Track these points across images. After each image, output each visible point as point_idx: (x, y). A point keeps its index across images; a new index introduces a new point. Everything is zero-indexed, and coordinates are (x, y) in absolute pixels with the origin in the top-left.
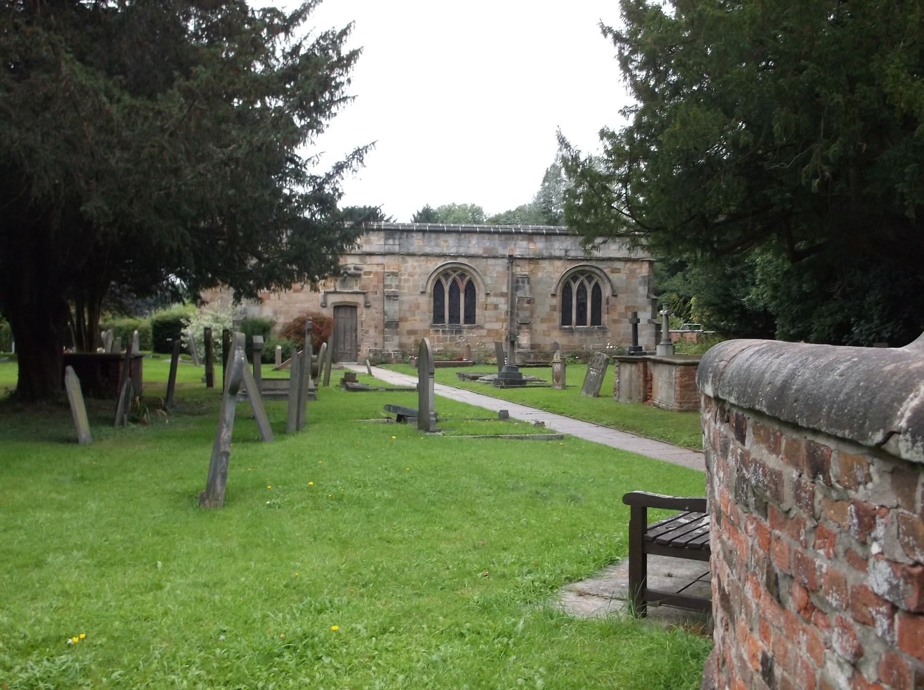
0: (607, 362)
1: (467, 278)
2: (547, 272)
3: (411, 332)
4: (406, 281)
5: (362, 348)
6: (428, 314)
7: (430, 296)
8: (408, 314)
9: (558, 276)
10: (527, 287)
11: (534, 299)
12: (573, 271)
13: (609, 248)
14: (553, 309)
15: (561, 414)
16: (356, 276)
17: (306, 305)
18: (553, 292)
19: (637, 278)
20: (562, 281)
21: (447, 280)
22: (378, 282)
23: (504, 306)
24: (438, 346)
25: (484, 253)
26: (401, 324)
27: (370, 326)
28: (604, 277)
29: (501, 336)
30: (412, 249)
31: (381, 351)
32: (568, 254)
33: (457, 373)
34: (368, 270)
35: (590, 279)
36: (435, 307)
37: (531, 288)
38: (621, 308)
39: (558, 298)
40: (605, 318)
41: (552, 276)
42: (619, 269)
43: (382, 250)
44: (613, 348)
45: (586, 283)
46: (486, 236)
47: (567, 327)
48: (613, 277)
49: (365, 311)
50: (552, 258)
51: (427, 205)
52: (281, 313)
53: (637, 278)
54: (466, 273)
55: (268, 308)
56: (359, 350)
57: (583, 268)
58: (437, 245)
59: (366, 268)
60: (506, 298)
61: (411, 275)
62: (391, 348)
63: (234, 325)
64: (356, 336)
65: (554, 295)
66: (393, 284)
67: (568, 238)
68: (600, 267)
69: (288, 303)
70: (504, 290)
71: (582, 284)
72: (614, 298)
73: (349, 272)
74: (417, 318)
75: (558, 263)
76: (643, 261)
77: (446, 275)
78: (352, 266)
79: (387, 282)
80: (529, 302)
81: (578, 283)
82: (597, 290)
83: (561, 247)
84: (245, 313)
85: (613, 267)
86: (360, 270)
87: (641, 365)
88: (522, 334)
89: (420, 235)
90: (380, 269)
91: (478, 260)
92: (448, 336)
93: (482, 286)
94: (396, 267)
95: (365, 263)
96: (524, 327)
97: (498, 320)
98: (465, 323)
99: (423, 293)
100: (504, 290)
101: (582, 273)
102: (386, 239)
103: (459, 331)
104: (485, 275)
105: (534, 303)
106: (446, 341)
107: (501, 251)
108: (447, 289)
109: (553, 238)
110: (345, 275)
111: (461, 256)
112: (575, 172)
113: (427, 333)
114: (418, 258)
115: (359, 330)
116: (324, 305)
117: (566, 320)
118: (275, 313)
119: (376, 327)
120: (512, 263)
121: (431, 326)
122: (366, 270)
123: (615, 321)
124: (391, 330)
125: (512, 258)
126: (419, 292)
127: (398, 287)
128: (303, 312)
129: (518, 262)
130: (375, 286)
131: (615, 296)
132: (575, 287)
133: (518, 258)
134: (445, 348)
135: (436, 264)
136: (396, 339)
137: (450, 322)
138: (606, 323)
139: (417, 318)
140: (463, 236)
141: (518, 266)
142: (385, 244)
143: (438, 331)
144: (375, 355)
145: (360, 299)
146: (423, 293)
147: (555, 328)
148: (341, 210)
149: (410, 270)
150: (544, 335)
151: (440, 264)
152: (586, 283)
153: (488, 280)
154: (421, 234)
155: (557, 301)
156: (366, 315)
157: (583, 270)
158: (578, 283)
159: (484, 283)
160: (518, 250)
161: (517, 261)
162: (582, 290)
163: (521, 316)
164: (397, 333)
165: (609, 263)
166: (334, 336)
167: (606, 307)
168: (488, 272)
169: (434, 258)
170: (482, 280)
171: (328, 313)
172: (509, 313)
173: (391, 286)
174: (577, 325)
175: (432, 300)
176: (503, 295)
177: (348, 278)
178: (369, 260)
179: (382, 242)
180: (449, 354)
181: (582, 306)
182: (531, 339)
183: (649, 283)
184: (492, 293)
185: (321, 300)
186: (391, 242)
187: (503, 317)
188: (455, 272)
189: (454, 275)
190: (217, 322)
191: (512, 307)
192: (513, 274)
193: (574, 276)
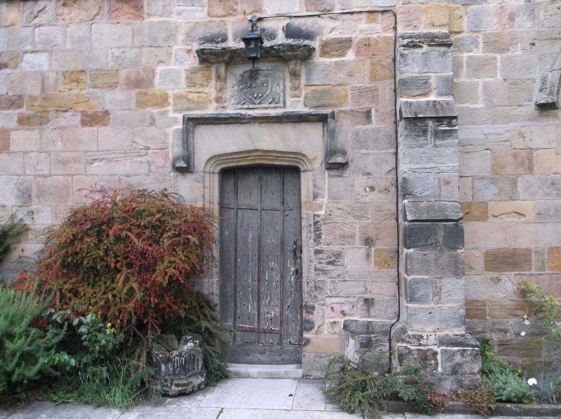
5: (316, 317)
22: (374, 78)
34: (335, 35)
52: (41, 194)
56: (307, 325)
64: (298, 273)
69: (65, 163)
86: (309, 36)
115: (307, 253)
119: (368, 241)
122: (327, 36)
124: (431, 254)
126: (531, 108)
130: (361, 92)
144: (367, 345)
156: (334, 198)
166: (222, 272)
177: (263, 66)
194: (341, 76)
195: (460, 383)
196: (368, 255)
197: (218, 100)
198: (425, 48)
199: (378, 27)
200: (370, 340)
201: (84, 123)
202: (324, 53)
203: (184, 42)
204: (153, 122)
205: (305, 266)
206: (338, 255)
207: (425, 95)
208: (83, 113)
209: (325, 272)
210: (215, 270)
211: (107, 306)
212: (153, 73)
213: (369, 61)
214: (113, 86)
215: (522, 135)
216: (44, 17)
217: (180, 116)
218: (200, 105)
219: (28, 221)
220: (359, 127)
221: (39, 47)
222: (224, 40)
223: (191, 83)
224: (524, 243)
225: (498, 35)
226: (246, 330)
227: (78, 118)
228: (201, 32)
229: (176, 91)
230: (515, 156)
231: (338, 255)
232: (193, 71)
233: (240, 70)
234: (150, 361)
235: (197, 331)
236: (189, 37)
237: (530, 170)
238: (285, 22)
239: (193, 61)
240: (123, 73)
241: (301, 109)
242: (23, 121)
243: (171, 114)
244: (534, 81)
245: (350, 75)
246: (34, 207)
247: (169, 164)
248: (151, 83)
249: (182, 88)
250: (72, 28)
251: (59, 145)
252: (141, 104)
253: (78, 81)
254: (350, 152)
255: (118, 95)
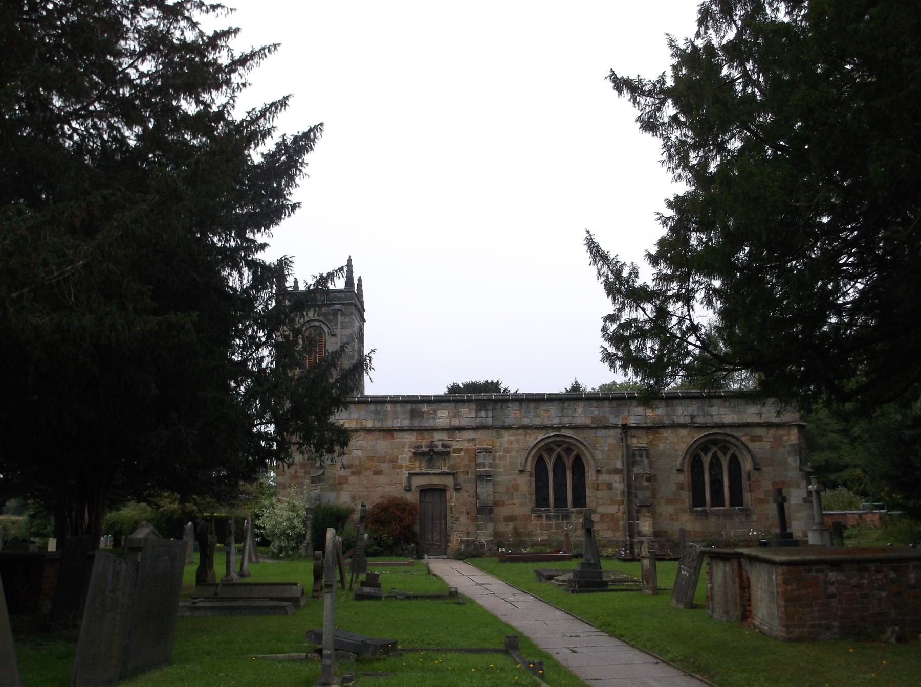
0: (703, 553)
1: (574, 453)
2: (669, 443)
3: (509, 519)
4: (501, 458)
6: (528, 497)
7: (531, 475)
8: (505, 498)
9: (684, 446)
10: (646, 461)
11: (655, 476)
12: (702, 441)
13: (745, 412)
14: (681, 487)
15: (620, 637)
16: (445, 455)
17: (388, 489)
18: (678, 466)
19: (784, 446)
20: (690, 453)
21: (550, 456)
22: (469, 461)
23: (619, 485)
24: (542, 535)
25: (592, 423)
26: (497, 510)
27: (461, 512)
28: (741, 447)
29: (618, 521)
30: (508, 421)
31: (474, 541)
32: (695, 420)
33: (535, 571)
34: (457, 447)
35: (725, 449)
36: (538, 488)
37: (651, 464)
38: (767, 485)
39: (686, 474)
40: (747, 497)
41: (677, 448)
42: (761, 436)
43: (473, 424)
44: (758, 535)
45: (720, 454)
46: (594, 404)
47: (699, 509)
48: (754, 446)
49: (454, 494)
50: (675, 426)
51: (576, 382)
53: (784, 446)
54: (573, 448)
55: (346, 493)
56: (449, 541)
57: (715, 437)
58: (537, 416)
59: (456, 445)
60: (621, 476)
61: (507, 451)
62: (485, 537)
63: (307, 514)
64: (446, 524)
65: (680, 471)
66: (486, 462)
67: (694, 402)
68: (736, 434)
69: (368, 487)
70: (619, 465)
71: (715, 456)
72: (756, 473)
73: (436, 450)
74: (516, 501)
75: (683, 432)
76: (790, 426)
77: (549, 449)
78: (439, 443)
79: (480, 460)
80: (648, 480)
81: (710, 455)
82: (735, 463)
83: (685, 413)
84: (319, 500)
85: (753, 434)
86: (449, 447)
87: (735, 563)
88: (641, 518)
89: (516, 406)
90: (471, 446)
91: (586, 431)
92: (553, 522)
93: (592, 462)
94: (490, 443)
95: (454, 440)
96: (644, 510)
97: (613, 502)
98: (574, 506)
99: (522, 472)
100: (619, 465)
101: (714, 442)
102: (478, 411)
103: (566, 517)
104: (595, 448)
105: (656, 480)
106: (551, 528)
107: (613, 420)
108: (550, 467)
109: (675, 402)
110: (431, 454)
111: (565, 428)
112: (619, 292)
113: (527, 518)
114: (515, 431)
115: (449, 518)
116: (408, 489)
117: (698, 500)
118: (354, 498)
119: (468, 513)
120: (626, 433)
121: (533, 511)
122: (455, 447)
123: (761, 501)
125: (625, 427)
126: (517, 471)
127: (491, 465)
128: (384, 497)
129: (634, 432)
130: (465, 466)
131: (758, 470)
132: (706, 460)
133: (634, 428)
134: (549, 537)
135: (536, 438)
136: (490, 528)
137: (556, 505)
138: (749, 503)
139: (516, 501)
140: (566, 405)
141: (634, 436)
142: (477, 417)
143: (540, 517)
144: (467, 546)
145: (449, 481)
146: (522, 472)
147: (684, 511)
148: (461, 385)
149: (505, 445)
150: (672, 519)
151: (540, 437)
152: (720, 454)
153: (599, 455)
154: (518, 404)
155: (683, 478)
157: (716, 439)
158: (710, 455)
159: (593, 457)
160: (632, 417)
161: (632, 430)
162: (715, 464)
163: (640, 496)
164: (491, 520)
165: (747, 430)
167: (748, 483)
168: (598, 445)
169: (534, 431)
170: (592, 454)
171: (412, 498)
172: (626, 493)
173: (483, 465)
174: (712, 506)
175: (533, 479)
176: (617, 471)
177: (434, 457)
178: (458, 435)
179: (473, 415)
180: (554, 544)
181: (717, 484)
182: (654, 524)
183: (800, 452)
184: (604, 469)
185: (405, 483)
186: (483, 414)
187: (619, 498)
188: (559, 446)
189: (559, 450)
190: (293, 511)
191: (629, 486)
192: (628, 447)
193: (704, 446)
194: (459, 460)
195: (491, 553)
196: (468, 518)
197: (420, 467)
198: (484, 453)
199: (471, 444)
200: (468, 545)
201: (374, 474)
202: (453, 453)
203: (408, 448)
204: (398, 474)
205: (448, 522)
206: (458, 518)
207: (484, 468)
208: (374, 471)
209: (454, 523)
210: (418, 523)
211: (389, 533)
212: (398, 458)
213: (468, 456)
214: (384, 462)
215: (515, 480)
216: (360, 438)
217: (407, 472)
218: (414, 469)
219: (355, 507)
220: (465, 477)
221: (359, 448)
222: (422, 447)
223: (410, 461)
224: (515, 513)
225: (507, 448)
226: (428, 544)
227: (372, 473)
228: (414, 445)
229: (406, 464)
230: (513, 486)
231: (458, 518)
232: (411, 458)
233: (427, 458)
234: (402, 549)
235: (414, 542)
236: (410, 446)
237: (517, 490)
238: (441, 442)
239: (411, 454)
240: (388, 458)
241: (447, 471)
242: (353, 473)
243: (404, 472)
244: (518, 462)
245: (462, 460)
246: (357, 502)
247: (403, 488)
248: (397, 462)
249: (407, 463)
250: (370, 442)
251: (366, 482)
252: (394, 468)
253: (372, 460)
254: (462, 485)
255: (386, 465)
